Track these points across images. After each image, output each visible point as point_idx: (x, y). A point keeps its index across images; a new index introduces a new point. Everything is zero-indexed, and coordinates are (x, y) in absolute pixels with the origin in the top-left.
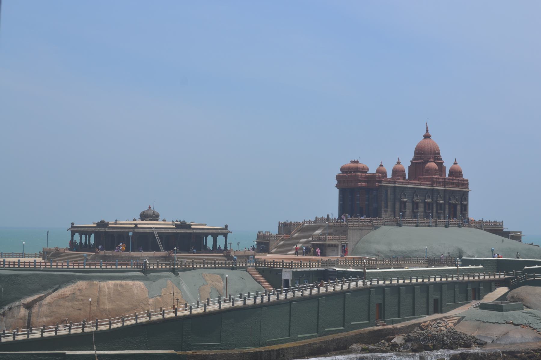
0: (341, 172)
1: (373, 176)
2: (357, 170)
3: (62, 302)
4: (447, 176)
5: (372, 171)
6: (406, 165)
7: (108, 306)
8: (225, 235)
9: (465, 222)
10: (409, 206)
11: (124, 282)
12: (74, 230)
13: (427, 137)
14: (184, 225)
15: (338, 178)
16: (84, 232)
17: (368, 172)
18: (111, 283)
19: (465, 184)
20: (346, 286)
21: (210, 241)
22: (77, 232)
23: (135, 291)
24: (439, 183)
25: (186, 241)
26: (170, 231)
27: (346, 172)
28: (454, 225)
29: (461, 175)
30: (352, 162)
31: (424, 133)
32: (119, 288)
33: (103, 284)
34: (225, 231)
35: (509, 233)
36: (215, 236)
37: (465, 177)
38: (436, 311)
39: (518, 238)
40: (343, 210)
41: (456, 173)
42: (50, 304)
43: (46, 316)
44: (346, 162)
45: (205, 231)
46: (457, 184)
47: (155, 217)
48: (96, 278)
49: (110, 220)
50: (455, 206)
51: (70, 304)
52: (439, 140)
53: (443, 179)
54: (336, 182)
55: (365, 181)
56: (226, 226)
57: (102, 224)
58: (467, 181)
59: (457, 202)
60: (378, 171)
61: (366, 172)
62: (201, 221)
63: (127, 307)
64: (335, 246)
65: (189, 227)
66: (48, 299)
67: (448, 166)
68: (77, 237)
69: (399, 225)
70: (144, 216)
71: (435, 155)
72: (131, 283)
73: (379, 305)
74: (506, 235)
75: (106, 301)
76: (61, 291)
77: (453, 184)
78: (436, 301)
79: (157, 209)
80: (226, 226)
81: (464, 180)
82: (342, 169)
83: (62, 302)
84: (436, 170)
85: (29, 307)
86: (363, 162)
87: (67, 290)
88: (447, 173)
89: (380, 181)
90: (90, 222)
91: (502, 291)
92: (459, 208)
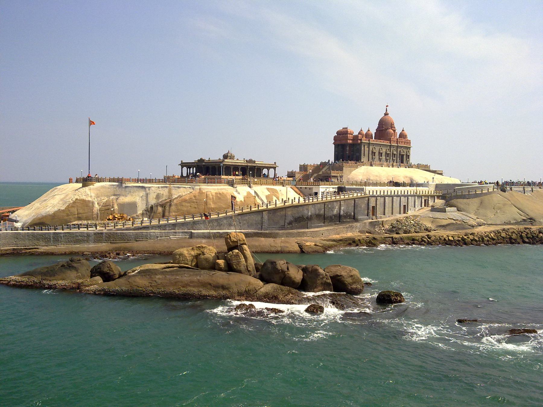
3: (184, 204)
5: (356, 133)
6: (373, 131)
7: (213, 206)
8: (275, 168)
10: (377, 154)
12: (183, 165)
13: (386, 114)
14: (251, 161)
15: (335, 138)
16: (188, 165)
19: (409, 142)
20: (355, 195)
21: (265, 171)
22: (185, 166)
25: (251, 172)
26: (243, 164)
32: (219, 195)
34: (275, 166)
37: (409, 138)
38: (404, 213)
40: (337, 158)
42: (176, 204)
43: (175, 212)
45: (263, 165)
47: (232, 157)
50: (403, 156)
51: (189, 204)
52: (393, 117)
56: (275, 163)
57: (201, 160)
60: (359, 133)
62: (260, 160)
63: (224, 206)
65: (254, 162)
68: (185, 169)
69: (371, 165)
70: (225, 157)
71: (392, 126)
73: (373, 207)
75: (211, 203)
78: (405, 206)
79: (233, 152)
80: (275, 163)
82: (337, 133)
83: (184, 204)
86: (350, 129)
88: (398, 137)
92: (405, 156)
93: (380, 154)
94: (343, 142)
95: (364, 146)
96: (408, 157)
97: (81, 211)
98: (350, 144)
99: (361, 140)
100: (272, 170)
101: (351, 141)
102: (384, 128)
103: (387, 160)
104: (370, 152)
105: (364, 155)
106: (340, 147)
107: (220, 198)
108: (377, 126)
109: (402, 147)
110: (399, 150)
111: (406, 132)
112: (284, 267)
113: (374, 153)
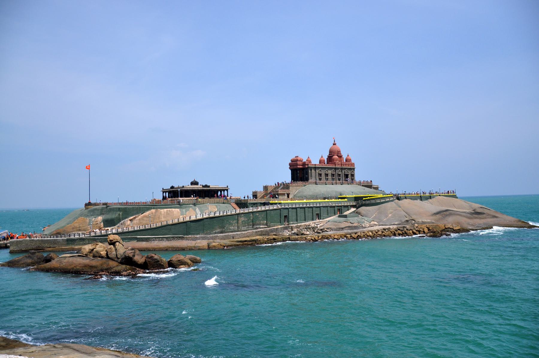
1: (305, 163)
6: (325, 158)
8: (227, 190)
11: (170, 209)
15: (290, 164)
18: (165, 210)
23: (175, 213)
31: (333, 142)
33: (162, 210)
36: (224, 190)
42: (139, 219)
44: (293, 157)
48: (159, 208)
49: (176, 186)
64: (284, 194)
65: (209, 186)
66: (139, 217)
67: (345, 157)
68: (164, 194)
72: (174, 209)
76: (144, 214)
82: (292, 161)
85: (130, 220)
87: (147, 213)
90: (168, 187)
91: (353, 210)
92: (350, 176)
93: (327, 175)
94: (295, 167)
95: (311, 170)
96: (353, 175)
97: (81, 226)
98: (300, 169)
99: (308, 165)
100: (226, 192)
101: (301, 167)
102: (333, 155)
103: (333, 179)
104: (317, 174)
107: (169, 214)
108: (328, 154)
109: (345, 169)
110: (343, 171)
111: (351, 157)
112: (131, 255)
113: (320, 175)
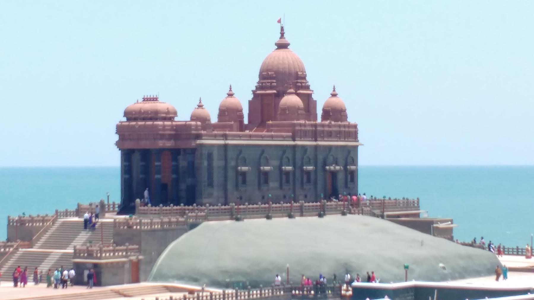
0: (125, 119)
2: (154, 116)
4: (319, 120)
5: (183, 116)
9: (354, 206)
15: (120, 129)
17: (176, 119)
24: (304, 135)
27: (135, 119)
28: (334, 210)
29: (345, 117)
30: (146, 100)
35: (431, 222)
39: (447, 234)
41: (335, 113)
46: (339, 135)
53: (312, 125)
54: (116, 138)
55: (171, 137)
58: (355, 126)
59: (338, 168)
61: (171, 119)
67: (321, 100)
74: (425, 226)
77: (330, 135)
81: (349, 126)
84: (299, 109)
88: (319, 112)
89: (199, 137)
105: (211, 185)
106: (136, 157)
